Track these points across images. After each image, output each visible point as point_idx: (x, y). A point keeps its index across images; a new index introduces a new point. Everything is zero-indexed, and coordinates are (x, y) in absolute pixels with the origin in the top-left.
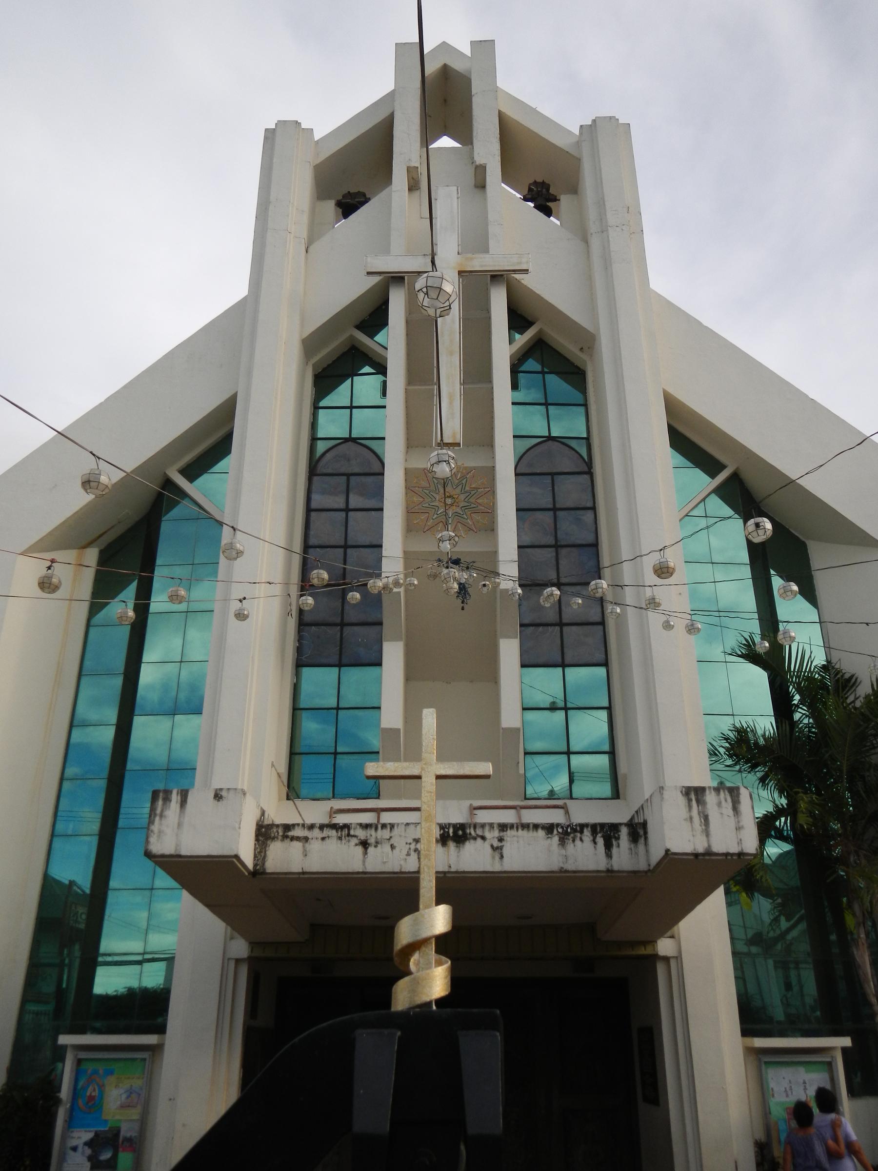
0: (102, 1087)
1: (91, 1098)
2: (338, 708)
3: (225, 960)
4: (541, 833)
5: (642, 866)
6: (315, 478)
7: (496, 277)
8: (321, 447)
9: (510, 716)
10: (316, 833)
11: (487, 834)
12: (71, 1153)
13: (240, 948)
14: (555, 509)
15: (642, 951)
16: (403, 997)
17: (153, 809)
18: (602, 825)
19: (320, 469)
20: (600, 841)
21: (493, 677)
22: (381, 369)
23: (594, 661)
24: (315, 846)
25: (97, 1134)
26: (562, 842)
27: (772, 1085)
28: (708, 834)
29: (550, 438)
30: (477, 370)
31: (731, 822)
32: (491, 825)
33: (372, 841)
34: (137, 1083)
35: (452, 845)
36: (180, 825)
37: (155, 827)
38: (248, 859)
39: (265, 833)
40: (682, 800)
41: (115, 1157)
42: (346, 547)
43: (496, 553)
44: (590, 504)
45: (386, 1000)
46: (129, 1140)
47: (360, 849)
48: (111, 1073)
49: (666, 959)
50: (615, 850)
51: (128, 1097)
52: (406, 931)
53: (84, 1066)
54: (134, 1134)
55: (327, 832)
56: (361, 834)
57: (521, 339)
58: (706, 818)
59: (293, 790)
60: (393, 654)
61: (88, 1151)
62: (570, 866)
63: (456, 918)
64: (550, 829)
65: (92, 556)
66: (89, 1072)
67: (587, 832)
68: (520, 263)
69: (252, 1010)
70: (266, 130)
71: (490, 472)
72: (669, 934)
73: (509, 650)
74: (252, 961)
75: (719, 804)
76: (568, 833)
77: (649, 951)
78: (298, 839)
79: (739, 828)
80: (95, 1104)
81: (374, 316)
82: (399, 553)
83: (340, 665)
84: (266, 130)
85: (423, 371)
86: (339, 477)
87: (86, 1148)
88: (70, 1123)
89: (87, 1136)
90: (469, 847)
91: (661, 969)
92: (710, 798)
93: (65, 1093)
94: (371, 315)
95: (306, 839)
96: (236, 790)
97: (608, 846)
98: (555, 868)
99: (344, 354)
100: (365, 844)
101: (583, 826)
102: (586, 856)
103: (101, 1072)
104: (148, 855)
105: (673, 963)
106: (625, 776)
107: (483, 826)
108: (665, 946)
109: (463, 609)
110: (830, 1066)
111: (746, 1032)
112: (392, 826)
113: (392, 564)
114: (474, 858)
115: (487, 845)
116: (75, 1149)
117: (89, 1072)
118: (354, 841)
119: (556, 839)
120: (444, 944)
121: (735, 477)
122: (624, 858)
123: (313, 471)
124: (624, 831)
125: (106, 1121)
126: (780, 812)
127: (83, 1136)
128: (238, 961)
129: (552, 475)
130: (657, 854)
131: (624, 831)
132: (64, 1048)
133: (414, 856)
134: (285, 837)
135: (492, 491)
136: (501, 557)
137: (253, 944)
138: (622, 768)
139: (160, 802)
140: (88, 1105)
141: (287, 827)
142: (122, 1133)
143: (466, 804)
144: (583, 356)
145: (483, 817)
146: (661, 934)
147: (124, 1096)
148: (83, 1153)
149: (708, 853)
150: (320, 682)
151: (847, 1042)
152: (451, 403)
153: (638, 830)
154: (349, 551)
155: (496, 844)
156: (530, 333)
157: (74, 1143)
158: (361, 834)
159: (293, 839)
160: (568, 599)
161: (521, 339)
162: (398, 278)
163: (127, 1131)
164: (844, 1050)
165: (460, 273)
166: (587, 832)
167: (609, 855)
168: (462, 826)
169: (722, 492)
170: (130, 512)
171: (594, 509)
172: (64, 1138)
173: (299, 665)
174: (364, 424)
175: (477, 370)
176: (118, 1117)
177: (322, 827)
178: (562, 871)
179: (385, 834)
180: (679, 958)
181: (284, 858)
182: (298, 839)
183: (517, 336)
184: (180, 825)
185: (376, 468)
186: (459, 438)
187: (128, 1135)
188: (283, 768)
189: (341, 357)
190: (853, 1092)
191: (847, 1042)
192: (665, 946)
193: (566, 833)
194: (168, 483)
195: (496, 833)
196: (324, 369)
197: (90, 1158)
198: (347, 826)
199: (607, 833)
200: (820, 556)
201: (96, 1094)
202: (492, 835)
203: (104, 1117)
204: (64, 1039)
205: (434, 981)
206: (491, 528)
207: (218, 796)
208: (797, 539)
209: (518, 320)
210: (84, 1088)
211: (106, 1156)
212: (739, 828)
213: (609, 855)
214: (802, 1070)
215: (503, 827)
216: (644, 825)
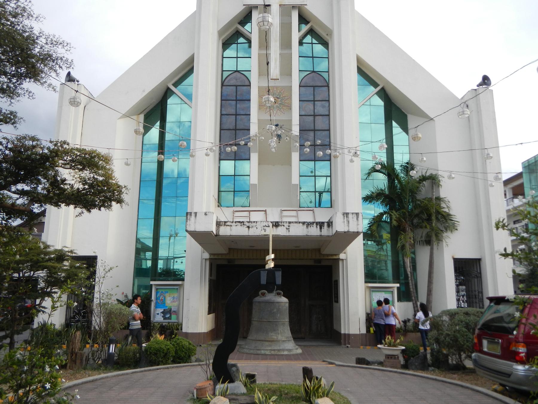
0: (165, 297)
1: (162, 300)
2: (235, 175)
3: (202, 259)
4: (301, 224)
5: (331, 234)
6: (224, 87)
7: (294, 7)
8: (226, 74)
9: (295, 180)
10: (234, 224)
11: (285, 225)
13: (207, 255)
14: (314, 101)
15: (335, 257)
16: (267, 267)
17: (187, 218)
18: (319, 222)
19: (225, 84)
20: (318, 227)
21: (290, 164)
22: (249, 42)
23: (326, 159)
24: (234, 228)
26: (307, 227)
27: (374, 297)
28: (348, 226)
29: (313, 72)
30: (286, 44)
31: (356, 223)
32: (286, 222)
33: (251, 226)
34: (176, 295)
35: (274, 227)
36: (195, 222)
37: (188, 223)
38: (215, 233)
39: (219, 224)
40: (342, 216)
41: (171, 316)
42: (236, 115)
43: (291, 120)
44: (327, 99)
45: (265, 267)
46: (175, 311)
47: (247, 229)
49: (343, 260)
50: (323, 230)
52: (267, 258)
53: (159, 290)
55: (237, 224)
56: (248, 224)
57: (305, 28)
58: (349, 222)
59: (219, 205)
60: (254, 157)
61: (162, 315)
62: (309, 234)
63: (275, 256)
64: (304, 223)
65: (142, 117)
67: (315, 224)
68: (304, 1)
69: (211, 275)
71: (290, 89)
72: (344, 252)
73: (295, 156)
74: (210, 259)
75: (353, 218)
76: (309, 224)
77: (337, 257)
78: (229, 225)
79: (358, 225)
80: (163, 302)
81: (246, 17)
82: (256, 121)
83: (235, 160)
85: (265, 43)
86: (234, 94)
88: (156, 307)
90: (279, 228)
91: (340, 262)
92: (350, 216)
93: (153, 297)
94: (244, 18)
95: (231, 226)
96: (205, 209)
97: (321, 228)
98: (305, 234)
99: (234, 34)
100: (249, 227)
101: (313, 223)
102: (314, 231)
104: (187, 231)
105: (344, 261)
106: (334, 201)
107: (284, 222)
108: (342, 256)
110: (392, 292)
111: (366, 282)
112: (257, 222)
113: (254, 129)
114: (281, 231)
115: (285, 228)
116: (158, 314)
118: (245, 226)
119: (305, 226)
120: (273, 260)
121: (383, 89)
122: (325, 232)
123: (222, 85)
124: (326, 224)
126: (385, 213)
128: (206, 259)
129: (314, 87)
130: (334, 232)
131: (326, 224)
132: (152, 285)
133: (263, 231)
134: (225, 225)
135: (290, 98)
136: (293, 123)
137: (210, 254)
138: (333, 199)
139: (189, 216)
140: (161, 303)
141: (225, 222)
143: (280, 209)
144: (326, 36)
145: (285, 219)
146: (341, 253)
149: (348, 232)
150: (228, 167)
151: (398, 285)
152: (276, 62)
153: (330, 224)
154: (237, 116)
155: (287, 227)
156: (309, 26)
157: (158, 312)
158: (248, 224)
159: (227, 225)
160: (317, 138)
161: (305, 28)
162: (256, 7)
164: (398, 288)
165: (280, 5)
166: (315, 224)
167: (321, 231)
168: (278, 222)
169: (378, 93)
170: (155, 101)
171: (329, 101)
172: (154, 311)
173: (220, 160)
174: (243, 65)
175: (286, 44)
177: (236, 222)
178: (307, 235)
179: (255, 224)
180: (346, 259)
181: (224, 231)
182: (229, 225)
183: (303, 26)
184: (195, 222)
185: (247, 83)
186: (278, 77)
188: (217, 197)
189: (233, 37)
190: (399, 300)
191: (398, 285)
192: (342, 256)
193: (309, 225)
194: (168, 89)
195: (288, 224)
196: (226, 41)
197: (163, 317)
198: (243, 222)
199: (321, 225)
200: (412, 121)
202: (286, 225)
204: (152, 283)
205: (271, 265)
206: (290, 108)
207: (206, 214)
208: (404, 113)
209: (303, 19)
210: (159, 297)
211: (168, 316)
212: (358, 225)
213: (321, 231)
214: (383, 293)
215: (290, 223)
216: (332, 222)
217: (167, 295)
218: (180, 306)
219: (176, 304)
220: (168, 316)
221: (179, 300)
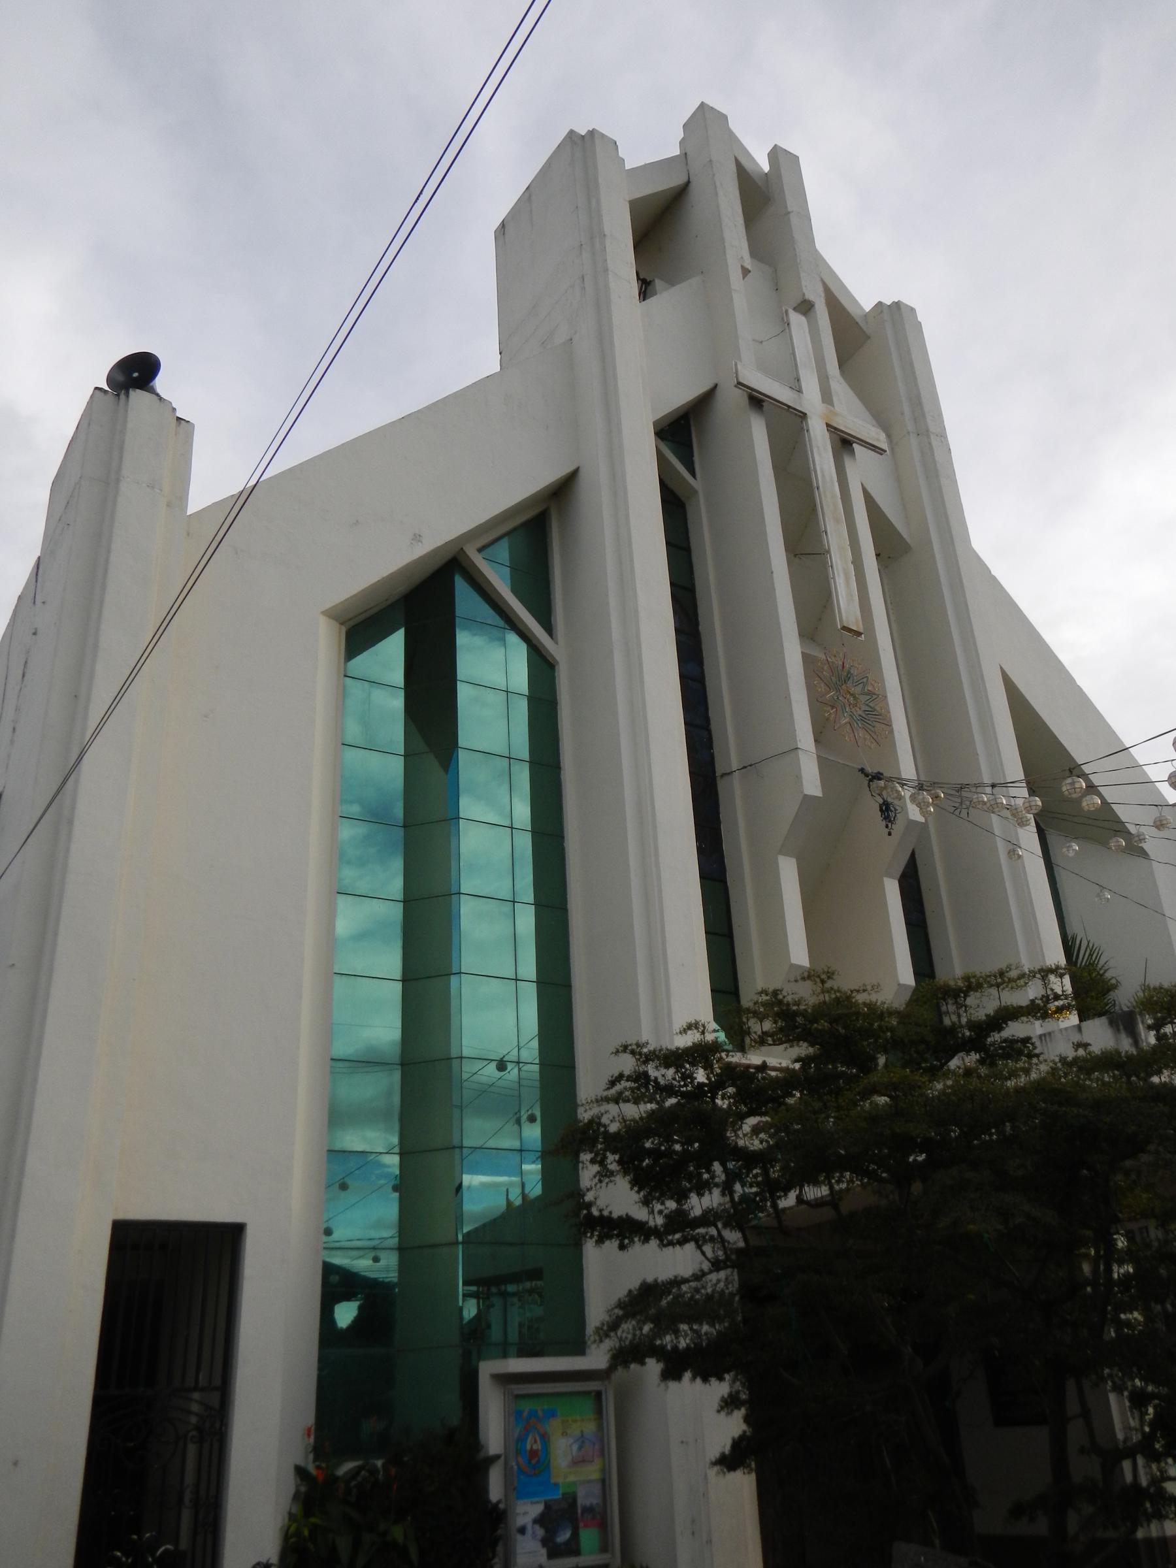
0: (545, 1437)
1: (533, 1453)
12: (519, 1537)
25: (548, 1506)
41: (575, 1535)
46: (589, 1510)
48: (554, 1415)
51: (580, 1448)
54: (595, 1501)
61: (540, 1532)
66: (525, 1414)
70: (572, 132)
84: (572, 132)
87: (537, 1527)
89: (536, 1510)
103: (540, 1413)
109: (890, 834)
116: (522, 1530)
117: (525, 1414)
125: (556, 1485)
127: (527, 1512)
140: (533, 1465)
142: (580, 1502)
147: (575, 1447)
148: (534, 1535)
163: (587, 1498)
176: (571, 1479)
187: (588, 1503)
201: (538, 1446)
203: (553, 1481)
211: (564, 1536)
217: (554, 1427)
218: (622, 1478)
219: (592, 1472)
220: (564, 1536)
221: (602, 1453)
